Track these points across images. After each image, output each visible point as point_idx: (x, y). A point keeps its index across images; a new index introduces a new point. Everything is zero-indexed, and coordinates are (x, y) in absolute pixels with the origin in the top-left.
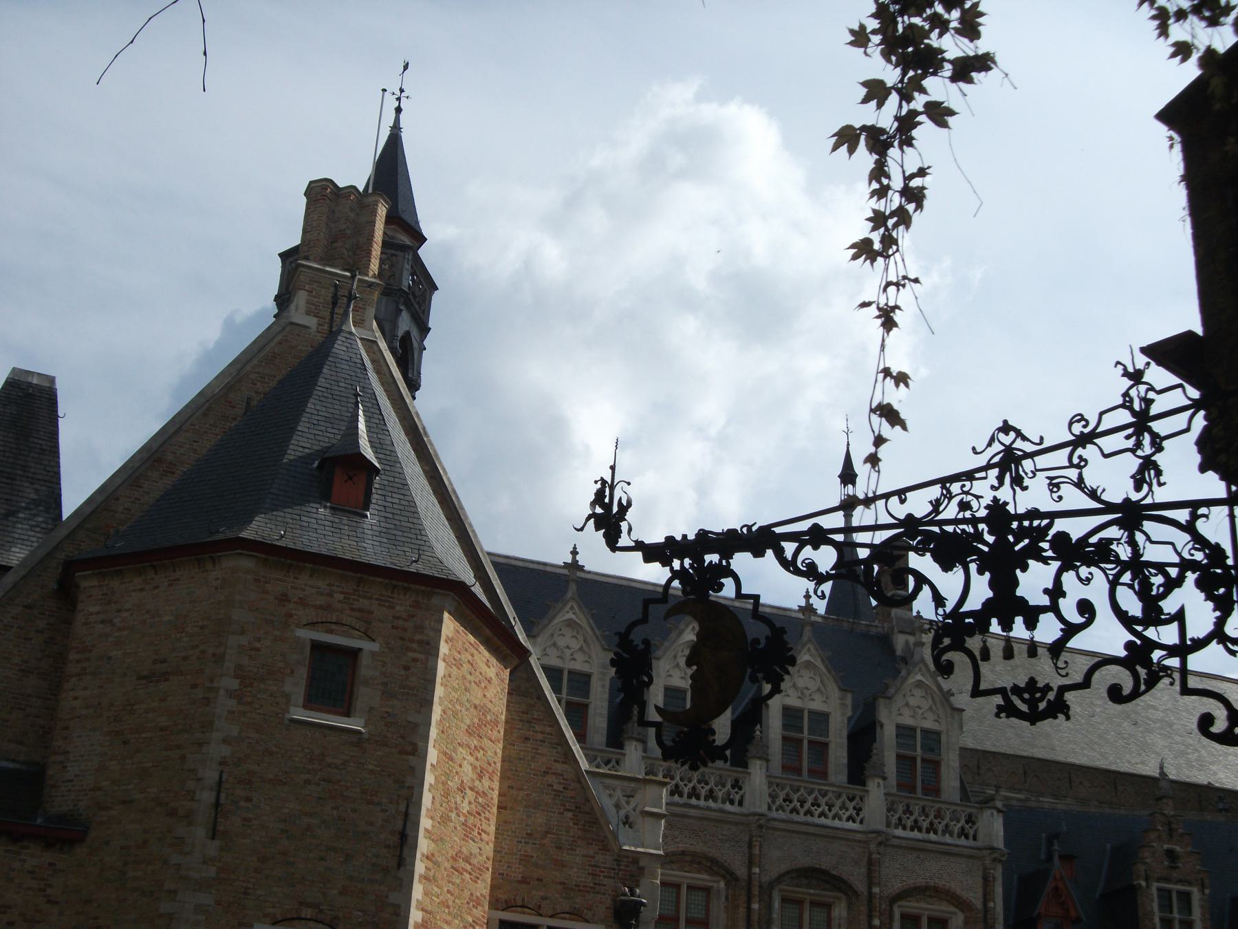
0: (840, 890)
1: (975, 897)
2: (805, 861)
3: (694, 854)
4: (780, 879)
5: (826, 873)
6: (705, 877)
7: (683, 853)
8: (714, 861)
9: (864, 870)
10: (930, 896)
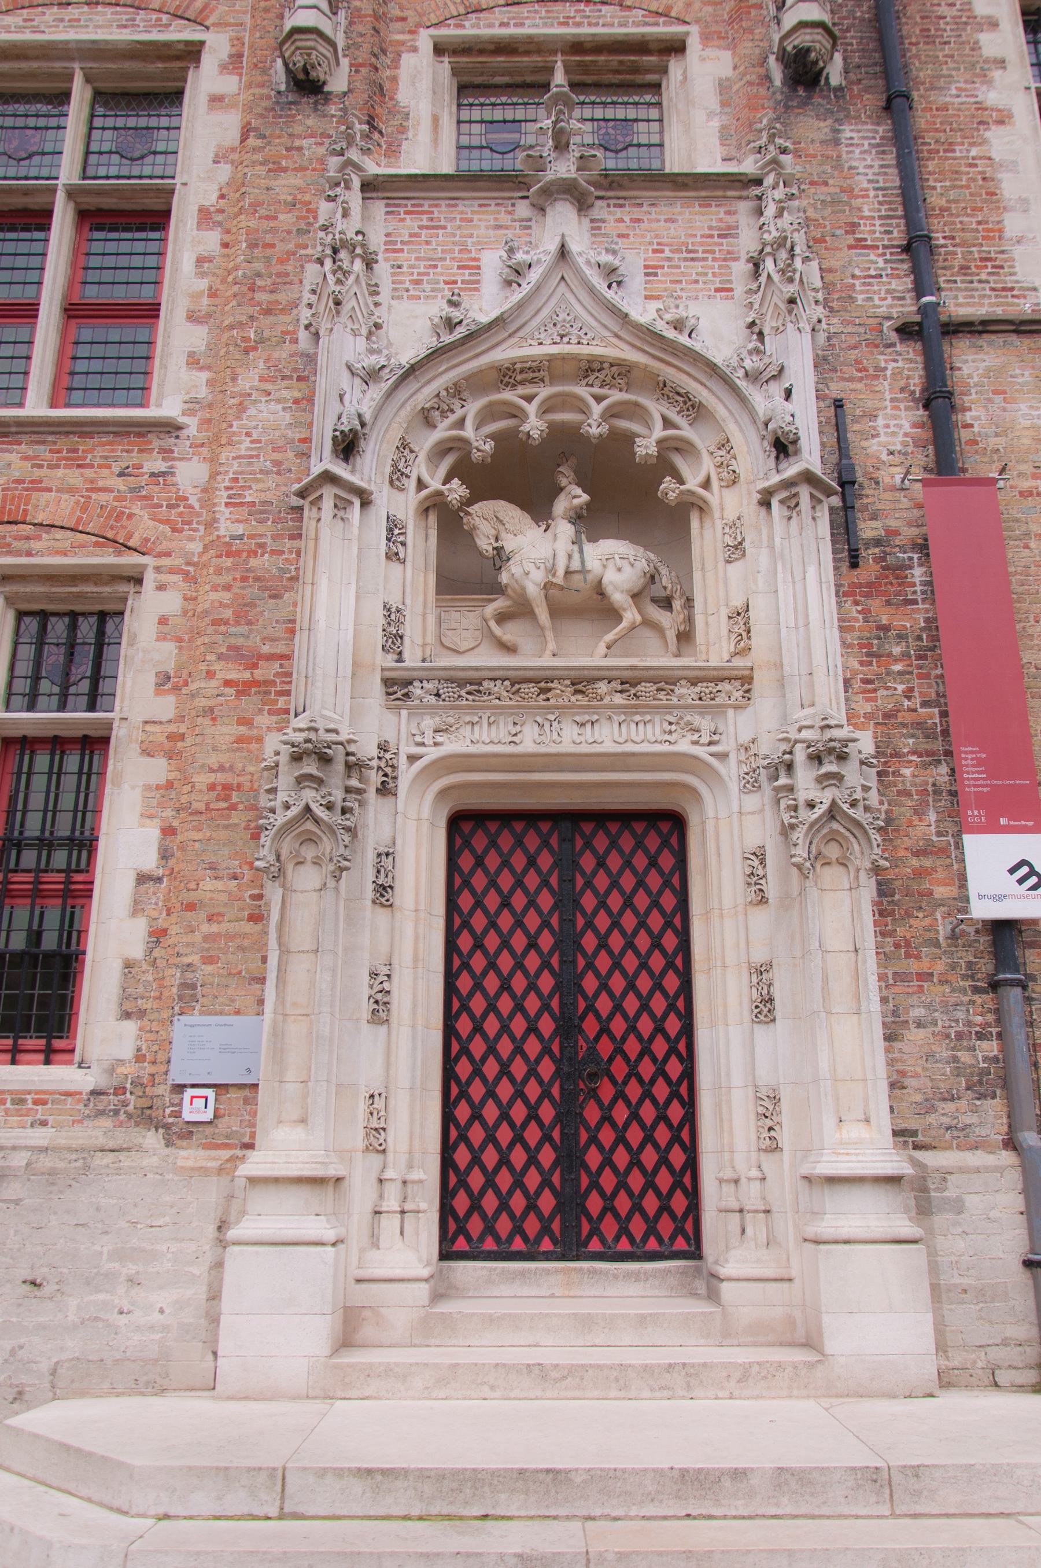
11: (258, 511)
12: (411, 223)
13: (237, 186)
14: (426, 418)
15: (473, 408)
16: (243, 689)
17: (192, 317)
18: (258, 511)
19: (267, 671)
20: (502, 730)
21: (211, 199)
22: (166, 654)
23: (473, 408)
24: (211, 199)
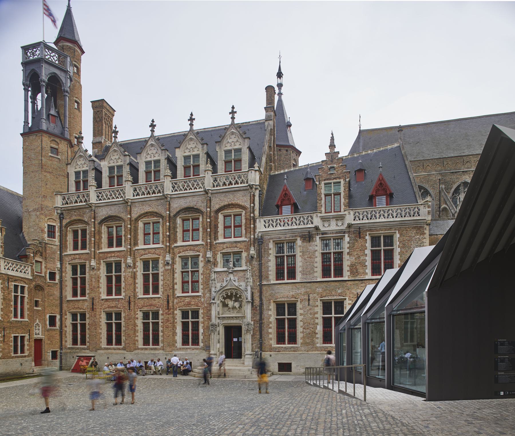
0: (199, 213)
1: (247, 205)
2: (185, 206)
3: (150, 212)
4: (178, 213)
5: (193, 208)
6: (156, 218)
7: (147, 213)
8: (156, 213)
9: (205, 204)
10: (232, 208)
11: (208, 304)
12: (218, 275)
13: (203, 271)
14: (221, 294)
15: (224, 292)
16: (208, 319)
17: (202, 285)
18: (208, 304)
19: (209, 317)
20: (227, 321)
21: (202, 272)
22: (202, 315)
23: (224, 292)
24: (202, 272)
